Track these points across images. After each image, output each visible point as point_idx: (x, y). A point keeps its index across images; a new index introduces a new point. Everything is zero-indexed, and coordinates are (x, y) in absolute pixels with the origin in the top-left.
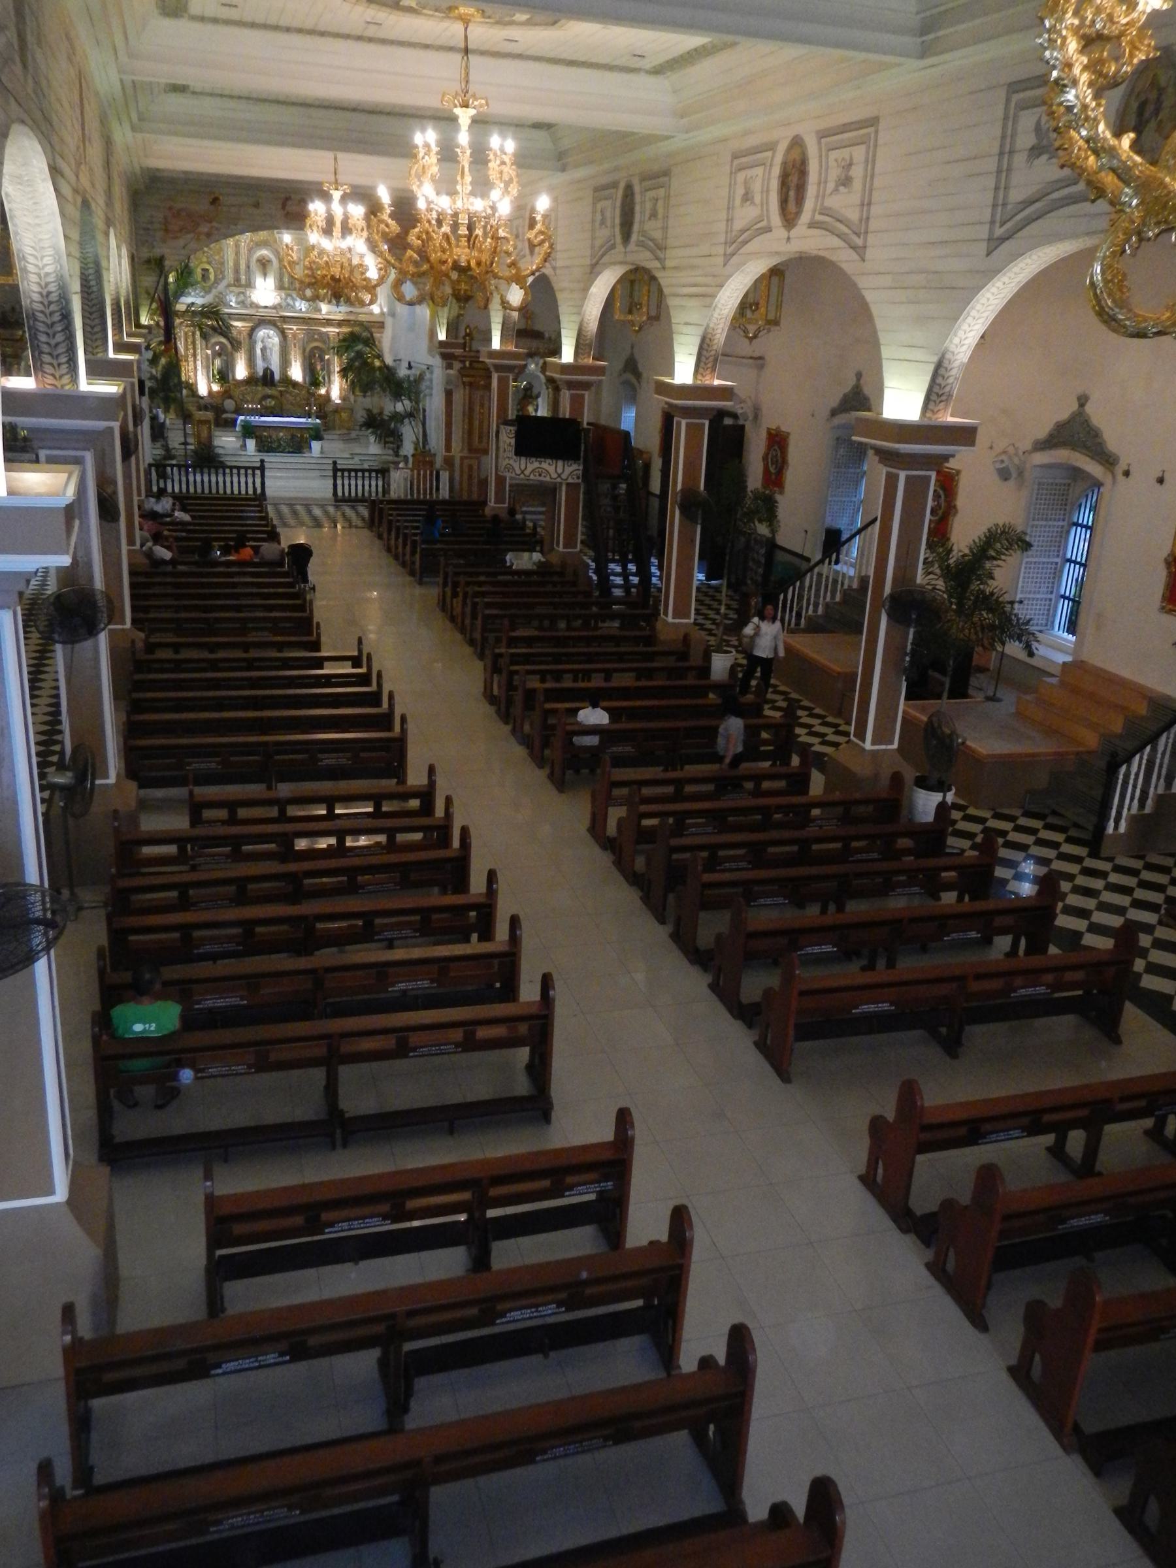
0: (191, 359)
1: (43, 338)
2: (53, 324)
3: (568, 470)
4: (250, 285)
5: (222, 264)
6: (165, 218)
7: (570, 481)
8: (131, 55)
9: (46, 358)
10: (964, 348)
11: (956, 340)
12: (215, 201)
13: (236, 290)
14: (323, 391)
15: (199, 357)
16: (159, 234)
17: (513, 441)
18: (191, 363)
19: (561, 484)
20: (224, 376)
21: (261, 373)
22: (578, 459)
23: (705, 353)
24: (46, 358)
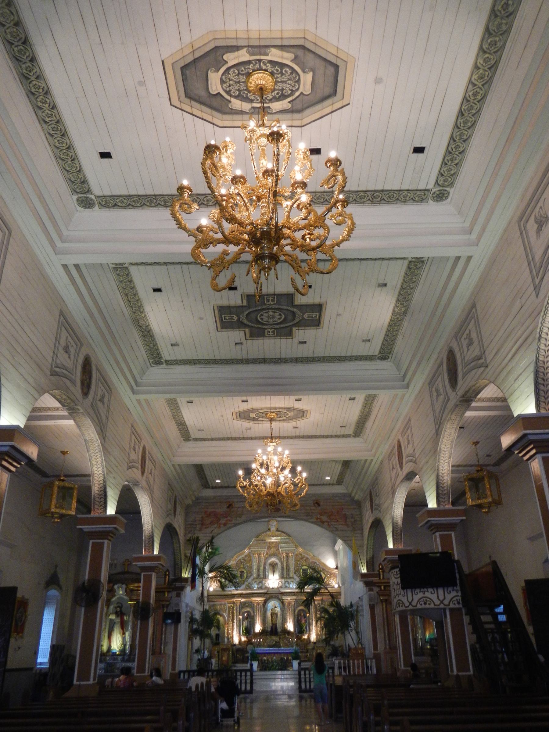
0: (231, 623)
3: (449, 597)
4: (265, 577)
5: (251, 568)
6: (202, 517)
7: (452, 606)
12: (230, 506)
13: (258, 581)
15: (235, 621)
16: (198, 527)
17: (399, 580)
18: (231, 625)
19: (445, 610)
20: (248, 631)
21: (269, 630)
22: (456, 585)
23: (542, 387)
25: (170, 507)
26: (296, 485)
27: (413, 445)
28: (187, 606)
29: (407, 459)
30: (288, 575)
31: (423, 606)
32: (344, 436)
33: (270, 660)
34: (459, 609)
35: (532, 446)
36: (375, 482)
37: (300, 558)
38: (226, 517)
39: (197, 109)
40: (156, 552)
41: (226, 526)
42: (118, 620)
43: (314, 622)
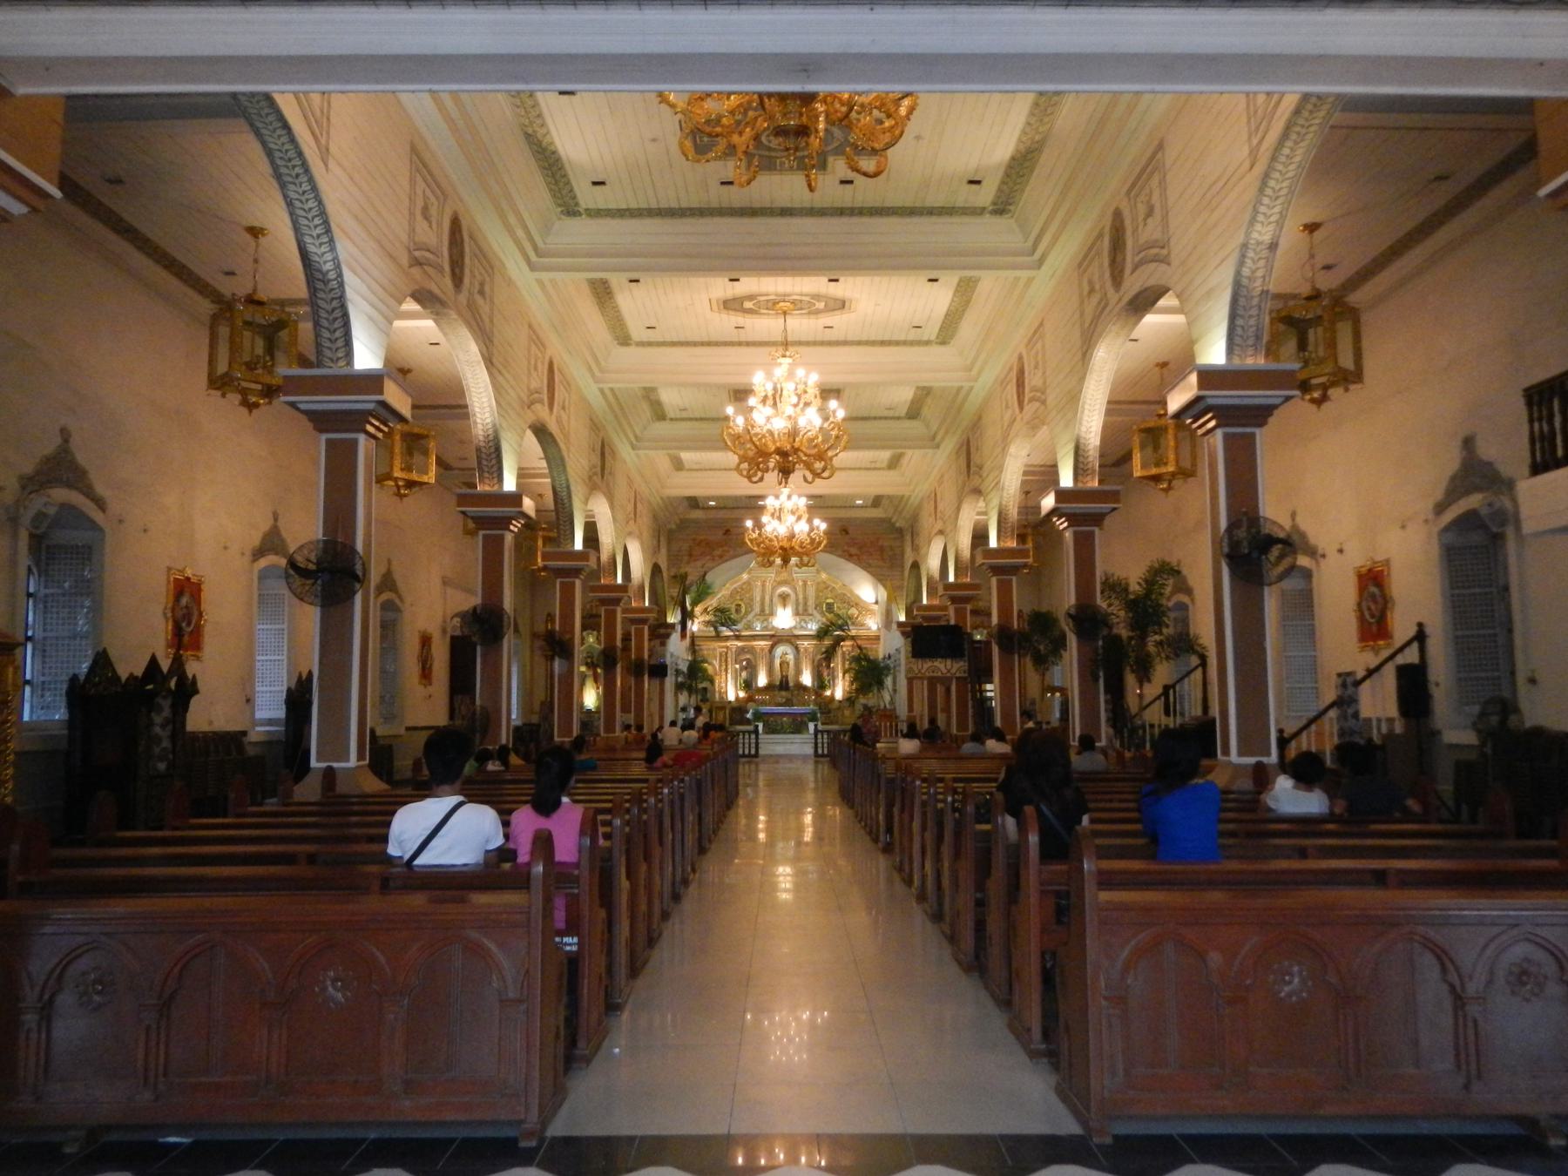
1: (485, 463)
2: (490, 454)
4: (772, 614)
5: (752, 600)
7: (958, 675)
8: (602, 371)
9: (486, 475)
10: (1093, 434)
11: (1084, 429)
12: (727, 532)
13: (762, 618)
14: (828, 693)
15: (729, 671)
16: (686, 558)
18: (724, 677)
19: (952, 679)
20: (748, 685)
21: (778, 683)
23: (1003, 525)
24: (486, 475)
25: (655, 542)
26: (813, 540)
27: (1044, 373)
28: (672, 655)
29: (1031, 395)
30: (805, 610)
31: (931, 674)
32: (875, 469)
33: (779, 722)
34: (965, 678)
35: (1210, 415)
36: (915, 519)
37: (823, 588)
38: (722, 546)
39: (731, 312)
40: (647, 604)
41: (722, 559)
42: (590, 673)
43: (841, 675)
